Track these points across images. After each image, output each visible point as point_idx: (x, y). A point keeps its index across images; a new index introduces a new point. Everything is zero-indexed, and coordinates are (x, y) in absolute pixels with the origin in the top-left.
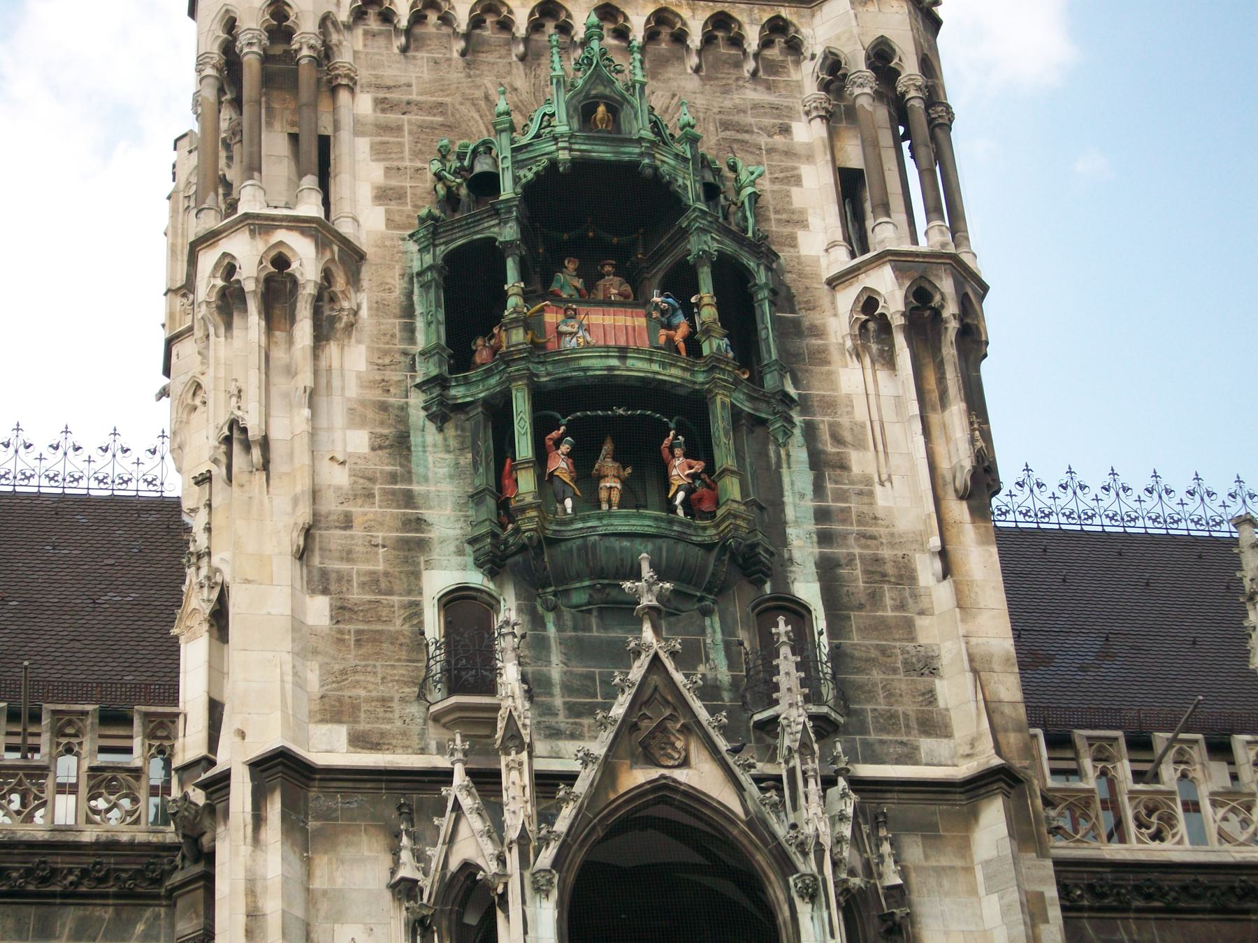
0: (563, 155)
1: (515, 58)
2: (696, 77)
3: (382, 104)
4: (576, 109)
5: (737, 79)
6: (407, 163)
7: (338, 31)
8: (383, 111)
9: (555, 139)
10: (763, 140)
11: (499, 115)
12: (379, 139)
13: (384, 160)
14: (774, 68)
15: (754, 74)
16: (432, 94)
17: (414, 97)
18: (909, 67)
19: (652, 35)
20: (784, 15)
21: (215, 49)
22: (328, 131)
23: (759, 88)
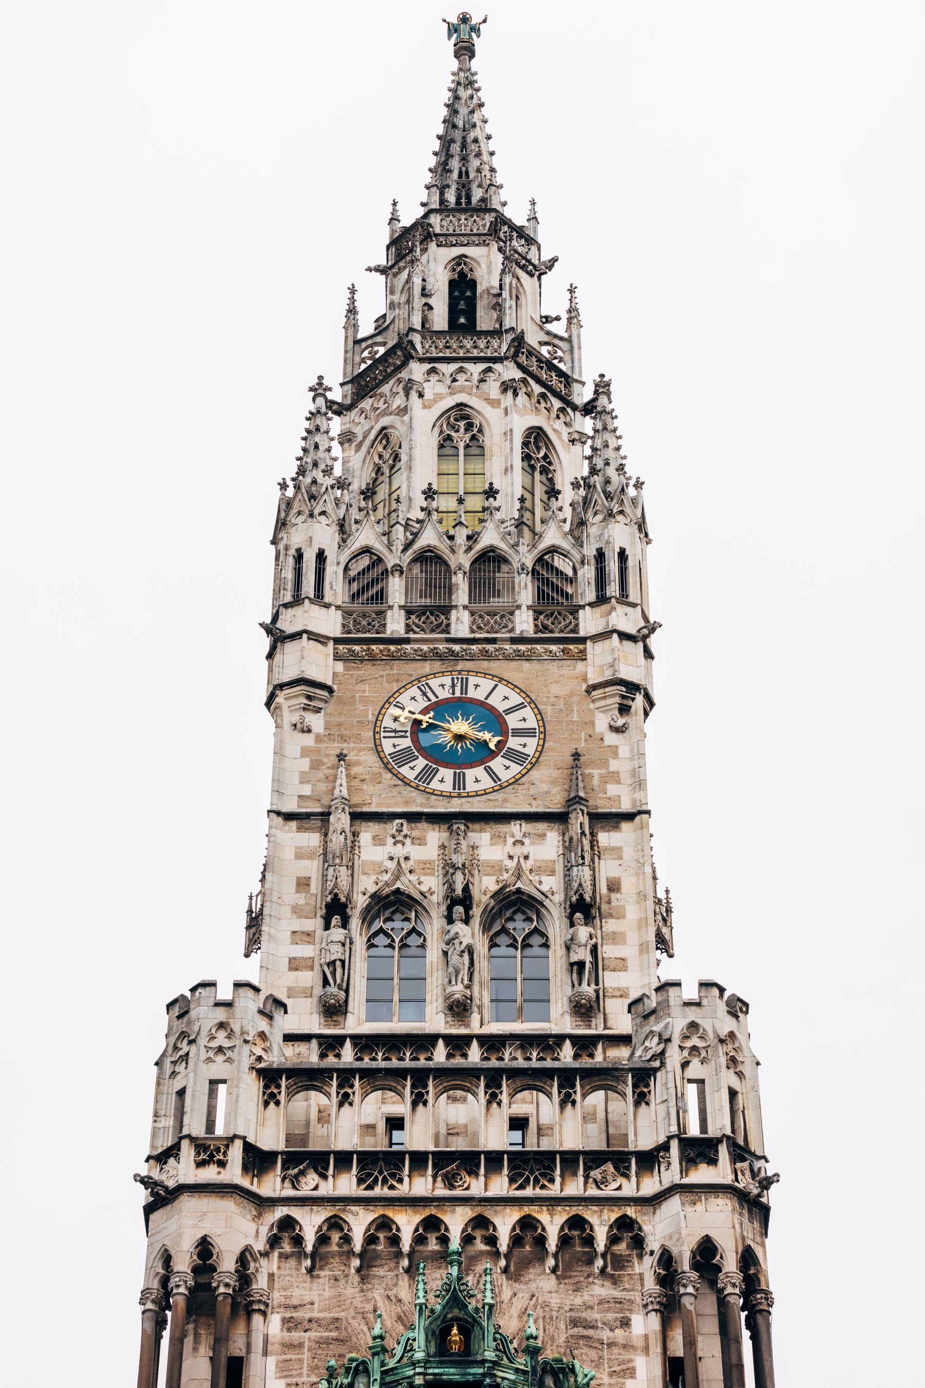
0: (419, 1381)
1: (401, 1271)
2: (553, 1277)
3: (289, 1324)
4: (433, 1333)
5: (588, 1276)
6: (305, 1379)
7: (255, 1260)
8: (289, 1330)
9: (414, 1364)
10: (606, 1335)
11: (374, 1338)
12: (284, 1357)
13: (286, 1376)
14: (620, 1262)
15: (603, 1271)
16: (329, 1310)
17: (316, 1314)
18: (730, 1264)
19: (516, 1241)
20: (629, 1213)
21: (155, 1284)
22: (243, 1353)
23: (606, 1283)
